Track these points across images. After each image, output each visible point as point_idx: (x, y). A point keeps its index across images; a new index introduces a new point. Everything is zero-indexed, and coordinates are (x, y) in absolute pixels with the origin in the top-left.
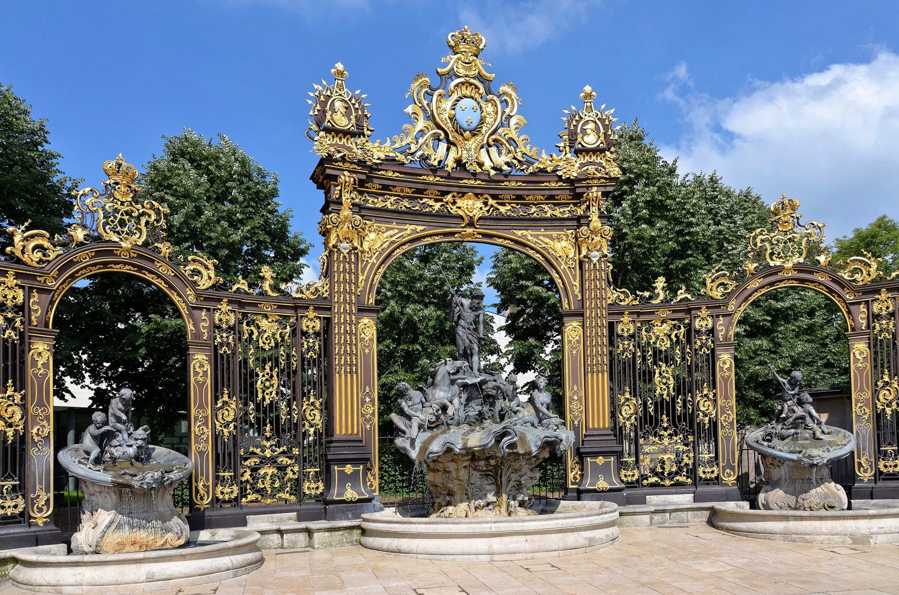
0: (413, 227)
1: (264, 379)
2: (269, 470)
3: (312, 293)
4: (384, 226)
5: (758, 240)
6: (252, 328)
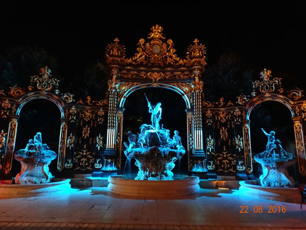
0: (137, 83)
1: (85, 130)
2: (84, 160)
3: (102, 104)
4: (127, 84)
5: (257, 84)
6: (83, 114)
